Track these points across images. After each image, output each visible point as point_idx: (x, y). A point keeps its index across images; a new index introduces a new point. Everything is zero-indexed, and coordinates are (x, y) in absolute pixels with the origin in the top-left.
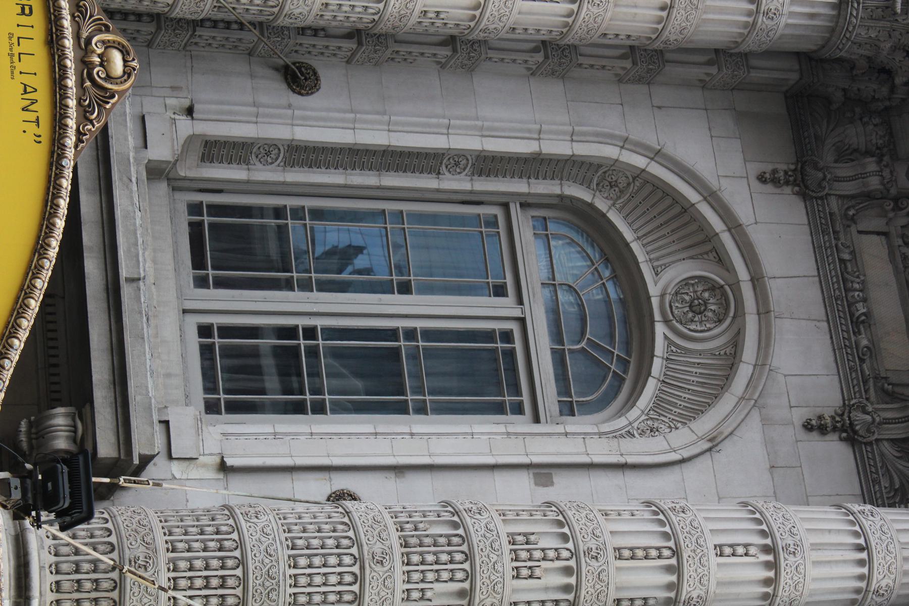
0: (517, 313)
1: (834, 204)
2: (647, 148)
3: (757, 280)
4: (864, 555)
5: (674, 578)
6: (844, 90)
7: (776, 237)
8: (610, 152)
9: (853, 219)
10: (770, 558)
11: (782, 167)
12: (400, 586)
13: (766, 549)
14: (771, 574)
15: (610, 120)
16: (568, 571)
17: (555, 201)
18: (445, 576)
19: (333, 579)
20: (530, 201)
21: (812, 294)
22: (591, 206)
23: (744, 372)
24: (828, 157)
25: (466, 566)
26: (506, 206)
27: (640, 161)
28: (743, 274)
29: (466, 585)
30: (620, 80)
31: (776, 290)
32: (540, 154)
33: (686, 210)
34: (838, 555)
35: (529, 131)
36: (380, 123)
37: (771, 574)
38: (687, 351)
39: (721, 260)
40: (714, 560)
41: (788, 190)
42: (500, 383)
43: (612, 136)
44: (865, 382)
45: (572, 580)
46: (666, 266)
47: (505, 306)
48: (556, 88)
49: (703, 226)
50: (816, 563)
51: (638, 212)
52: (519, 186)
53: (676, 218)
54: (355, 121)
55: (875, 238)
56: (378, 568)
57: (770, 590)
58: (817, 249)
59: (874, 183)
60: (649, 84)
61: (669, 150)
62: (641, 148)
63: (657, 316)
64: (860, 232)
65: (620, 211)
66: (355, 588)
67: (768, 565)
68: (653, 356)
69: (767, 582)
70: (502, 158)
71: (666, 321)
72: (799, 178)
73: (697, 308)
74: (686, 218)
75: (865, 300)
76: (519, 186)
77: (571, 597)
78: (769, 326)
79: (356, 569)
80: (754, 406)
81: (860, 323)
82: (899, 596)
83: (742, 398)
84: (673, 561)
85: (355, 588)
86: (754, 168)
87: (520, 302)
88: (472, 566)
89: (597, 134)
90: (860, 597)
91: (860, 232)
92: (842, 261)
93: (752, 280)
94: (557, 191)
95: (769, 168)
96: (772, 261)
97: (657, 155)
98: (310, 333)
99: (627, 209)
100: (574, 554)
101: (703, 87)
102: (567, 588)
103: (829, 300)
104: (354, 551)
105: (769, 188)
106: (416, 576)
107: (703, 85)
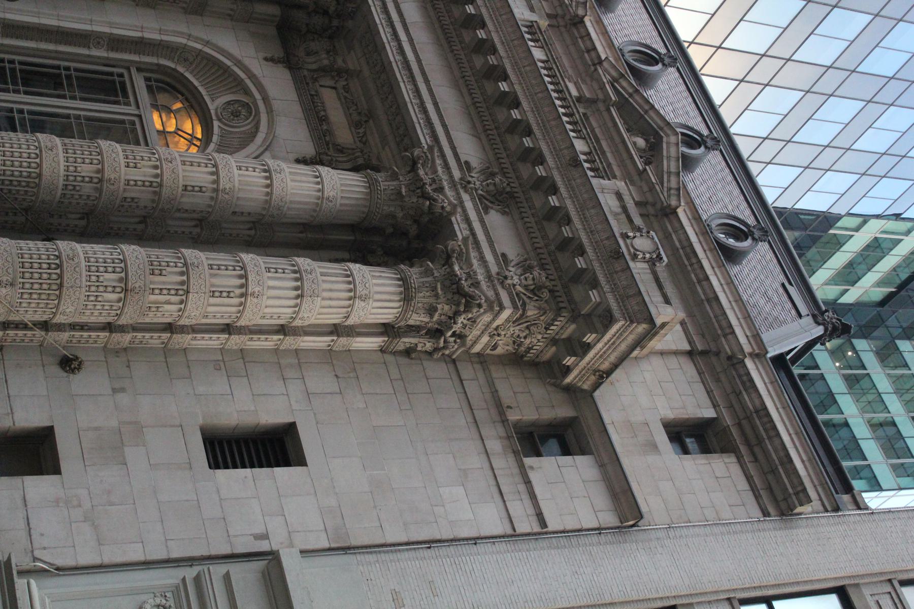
0: (136, 112)
1: (306, 73)
2: (202, 40)
3: (266, 99)
4: (319, 179)
5: (215, 177)
6: (307, 25)
7: (277, 84)
8: (184, 41)
9: (315, 80)
10: (267, 174)
11: (276, 56)
12: (62, 163)
13: (265, 171)
14: (269, 182)
15: (183, 28)
16: (156, 167)
17: (155, 68)
18: (87, 161)
19: (25, 155)
20: (143, 66)
21: (296, 109)
22: (175, 70)
23: (260, 137)
24: (301, 53)
25: (99, 157)
26: (128, 69)
27: (199, 46)
28: (258, 96)
29: (100, 166)
30: (186, 13)
31: (276, 105)
32: (142, 38)
33: (226, 70)
34: (304, 178)
35: (136, 26)
36: (53, 15)
37: (269, 182)
38: (232, 132)
39: (247, 92)
40: (236, 172)
41: (280, 65)
42: (116, 90)
43: (182, 33)
44: (327, 145)
45: (159, 171)
46: (217, 97)
47: (132, 110)
48: (153, 11)
49: (236, 78)
50: (292, 181)
51: (201, 73)
52: (136, 58)
53: (220, 73)
54: (39, 13)
55: (329, 90)
56: (50, 152)
57: (269, 190)
58: (298, 89)
59: (326, 62)
60: (202, 15)
61: (214, 41)
62: (197, 39)
63: (214, 117)
64: (321, 86)
65: (191, 73)
66: (38, 160)
67: (266, 178)
68: (213, 134)
69: (268, 186)
70: (123, 41)
71: (219, 120)
72: (288, 61)
73: (236, 114)
74: (227, 75)
75: (325, 111)
76: (136, 58)
77: (159, 180)
78: (273, 116)
79: (37, 152)
80: (266, 149)
81: (323, 119)
82: (341, 205)
83: (261, 146)
84: (214, 169)
85: (38, 160)
86: (262, 55)
87: (138, 107)
88: (102, 158)
89: (175, 31)
90: (319, 202)
91: (321, 86)
92: (311, 95)
93: (263, 99)
94: (156, 62)
95: (269, 56)
96: (272, 92)
97: (207, 43)
98: (21, 111)
99: (195, 72)
100: (159, 160)
101: (232, 20)
102: (156, 176)
103: (305, 110)
104: (36, 144)
105: (270, 63)
106: (71, 160)
107: (231, 17)
